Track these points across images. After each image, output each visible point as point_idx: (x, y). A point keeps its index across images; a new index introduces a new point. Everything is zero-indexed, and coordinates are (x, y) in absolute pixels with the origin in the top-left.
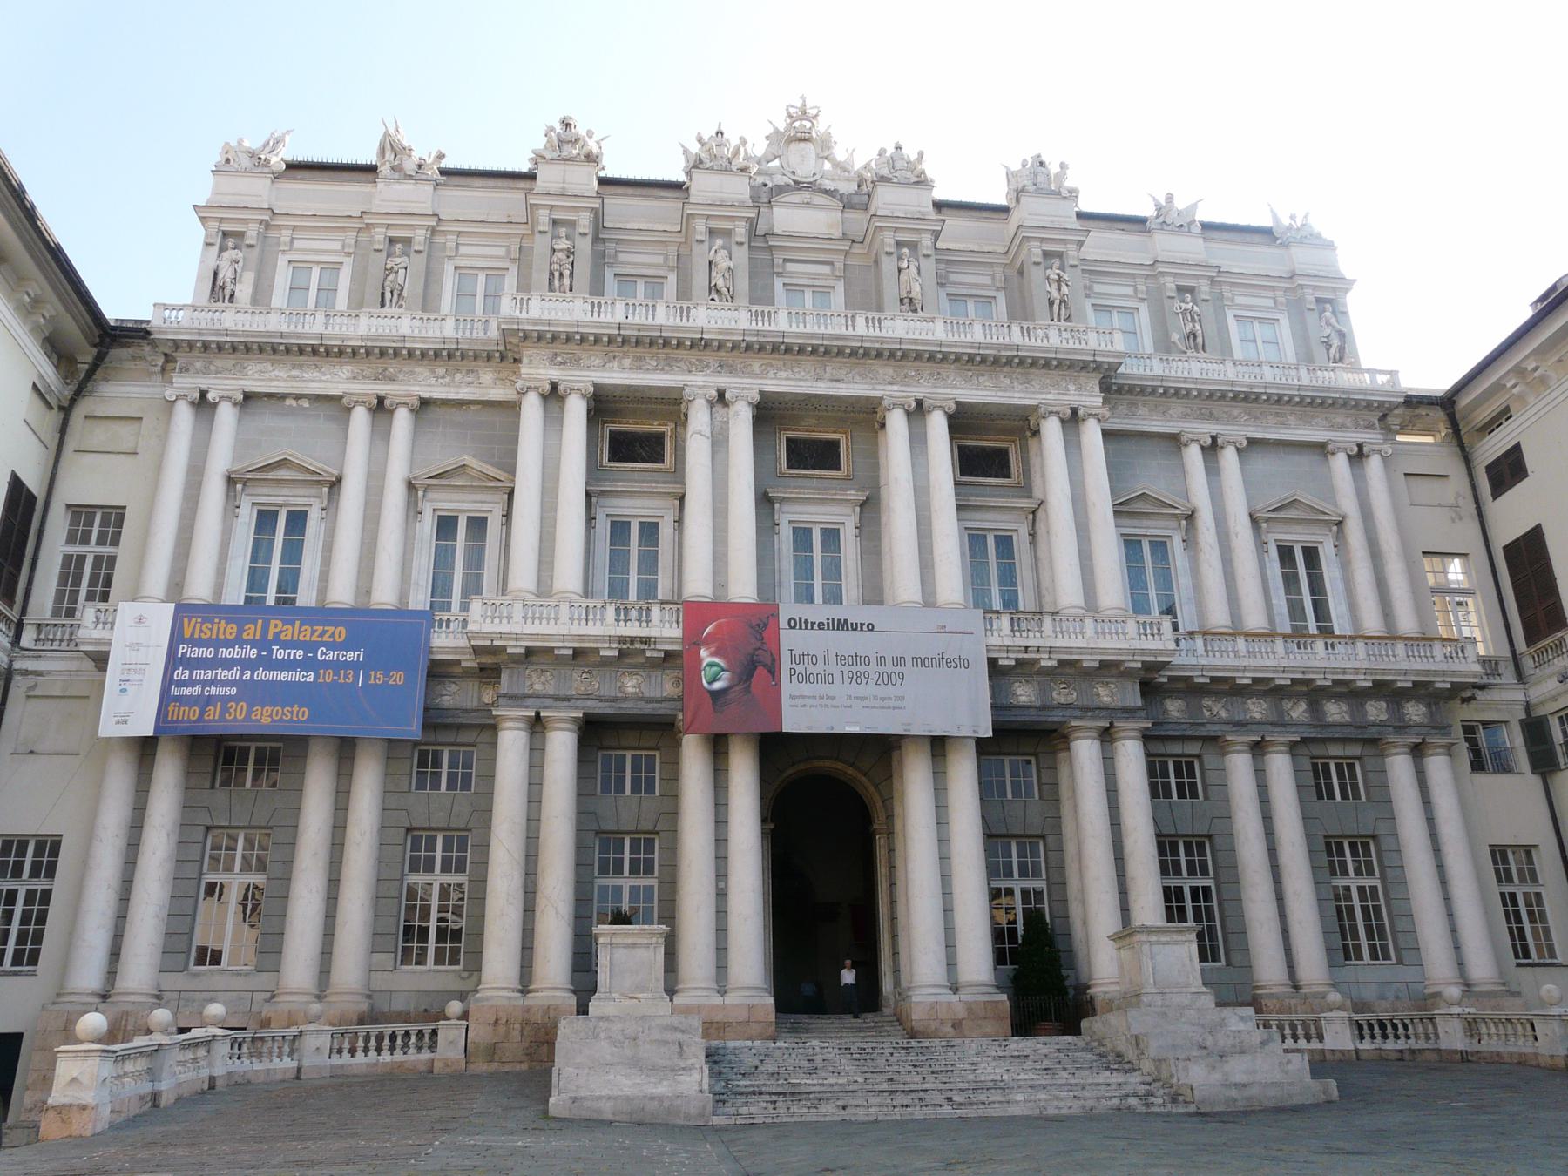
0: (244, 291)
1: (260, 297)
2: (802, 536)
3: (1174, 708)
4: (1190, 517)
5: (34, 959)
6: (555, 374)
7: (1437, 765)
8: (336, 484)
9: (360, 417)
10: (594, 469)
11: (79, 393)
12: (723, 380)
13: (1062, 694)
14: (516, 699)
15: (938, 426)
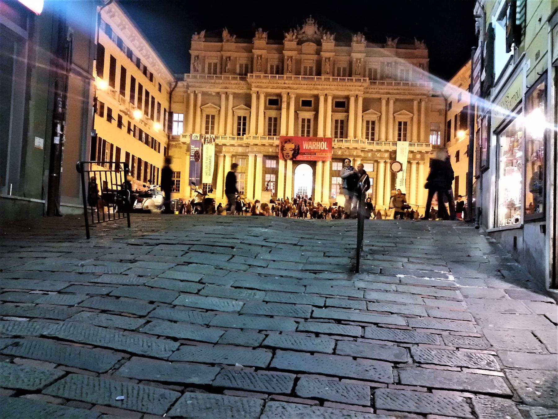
0: (200, 69)
1: (203, 71)
2: (303, 120)
3: (370, 155)
4: (380, 117)
5: (179, 191)
6: (257, 89)
7: (421, 167)
8: (219, 111)
9: (223, 96)
10: (266, 108)
11: (173, 90)
12: (289, 90)
13: (347, 153)
14: (252, 152)
15: (330, 99)
